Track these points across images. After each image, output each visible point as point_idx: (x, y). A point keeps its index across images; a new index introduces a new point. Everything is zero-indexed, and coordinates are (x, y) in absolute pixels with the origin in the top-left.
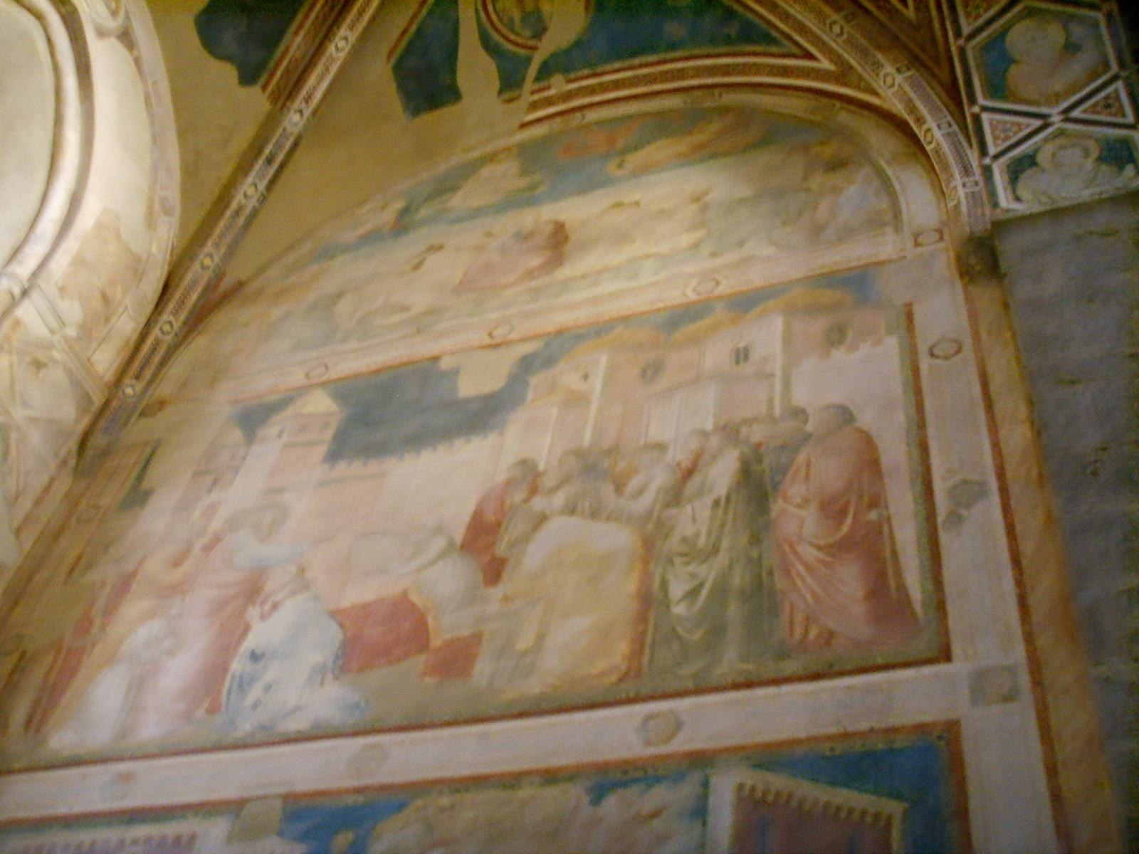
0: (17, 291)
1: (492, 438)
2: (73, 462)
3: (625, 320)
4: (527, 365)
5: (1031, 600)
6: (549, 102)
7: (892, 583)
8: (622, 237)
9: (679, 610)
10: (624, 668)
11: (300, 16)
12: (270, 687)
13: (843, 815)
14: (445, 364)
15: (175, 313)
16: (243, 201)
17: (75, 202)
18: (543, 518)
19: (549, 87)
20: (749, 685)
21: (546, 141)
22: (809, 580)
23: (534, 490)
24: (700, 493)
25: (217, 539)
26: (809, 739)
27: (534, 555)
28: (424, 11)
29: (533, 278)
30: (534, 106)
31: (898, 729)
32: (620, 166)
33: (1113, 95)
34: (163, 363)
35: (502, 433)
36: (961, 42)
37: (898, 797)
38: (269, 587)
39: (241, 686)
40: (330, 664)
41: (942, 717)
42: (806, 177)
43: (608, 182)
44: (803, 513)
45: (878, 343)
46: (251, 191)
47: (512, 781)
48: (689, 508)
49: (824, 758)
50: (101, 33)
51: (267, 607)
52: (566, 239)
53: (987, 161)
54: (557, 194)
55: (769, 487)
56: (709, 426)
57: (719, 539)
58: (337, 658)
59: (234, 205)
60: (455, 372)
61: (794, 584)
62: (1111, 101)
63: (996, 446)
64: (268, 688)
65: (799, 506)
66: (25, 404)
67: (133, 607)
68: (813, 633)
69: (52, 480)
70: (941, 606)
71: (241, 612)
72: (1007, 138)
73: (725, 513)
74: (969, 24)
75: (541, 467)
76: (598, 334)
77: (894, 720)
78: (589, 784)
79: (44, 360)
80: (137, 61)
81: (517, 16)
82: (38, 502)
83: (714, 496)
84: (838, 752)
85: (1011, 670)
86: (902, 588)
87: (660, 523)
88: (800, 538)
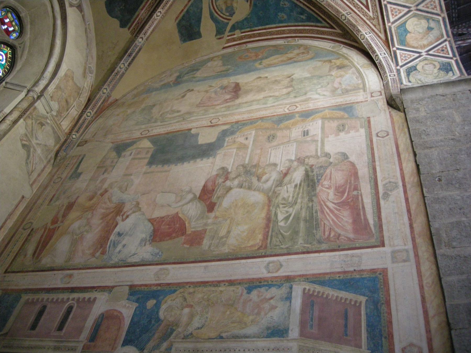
0: (36, 97)
1: (211, 159)
2: (52, 161)
3: (262, 119)
4: (224, 134)
5: (415, 225)
6: (234, 40)
7: (362, 218)
8: (260, 90)
9: (282, 224)
10: (260, 244)
11: (144, 4)
12: (125, 245)
13: (343, 301)
14: (193, 132)
15: (92, 109)
16: (119, 69)
17: (58, 66)
18: (230, 189)
19: (234, 35)
20: (308, 252)
21: (233, 53)
22: (331, 215)
23: (227, 179)
24: (290, 182)
25: (106, 191)
26: (330, 273)
27: (226, 202)
28: (190, 3)
29: (227, 102)
30: (228, 41)
31: (364, 270)
32: (260, 64)
33: (445, 47)
34: (87, 127)
35: (214, 157)
36: (390, 24)
37: (364, 295)
38: (125, 210)
39: (114, 244)
40: (148, 238)
41: (381, 267)
42: (330, 70)
43: (256, 69)
44: (329, 191)
45: (358, 131)
46: (122, 66)
47: (217, 284)
48: (286, 187)
49: (336, 280)
50: (71, 5)
51: (124, 217)
52: (240, 89)
53: (398, 68)
54: (235, 73)
55: (316, 181)
56: (293, 158)
57: (297, 199)
58: (151, 236)
59: (116, 71)
60: (197, 135)
61: (326, 216)
62: (444, 49)
63: (401, 169)
64: (124, 246)
65: (327, 188)
66: (37, 139)
67: (73, 215)
68: (332, 235)
69: (45, 167)
70: (381, 227)
71: (114, 219)
72: (406, 60)
73: (299, 189)
74: (393, 18)
75: (229, 170)
76: (251, 123)
77: (363, 267)
78: (246, 286)
79: (44, 123)
80: (83, 16)
81: (224, 7)
82: (39, 175)
83: (295, 183)
84: (341, 278)
85: (407, 251)
86: (366, 219)
87: (274, 192)
88: (328, 200)
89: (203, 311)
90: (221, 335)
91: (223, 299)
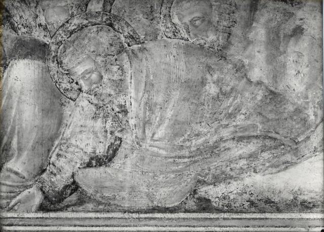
89: (102, 77)
90: (203, 191)
91: (176, 20)
